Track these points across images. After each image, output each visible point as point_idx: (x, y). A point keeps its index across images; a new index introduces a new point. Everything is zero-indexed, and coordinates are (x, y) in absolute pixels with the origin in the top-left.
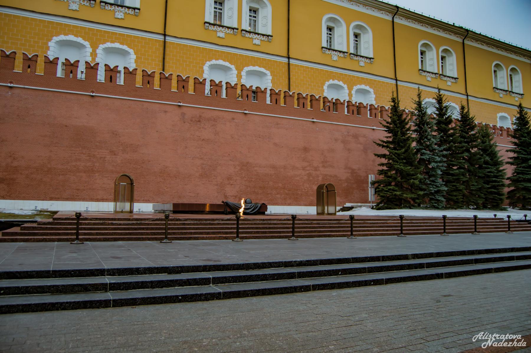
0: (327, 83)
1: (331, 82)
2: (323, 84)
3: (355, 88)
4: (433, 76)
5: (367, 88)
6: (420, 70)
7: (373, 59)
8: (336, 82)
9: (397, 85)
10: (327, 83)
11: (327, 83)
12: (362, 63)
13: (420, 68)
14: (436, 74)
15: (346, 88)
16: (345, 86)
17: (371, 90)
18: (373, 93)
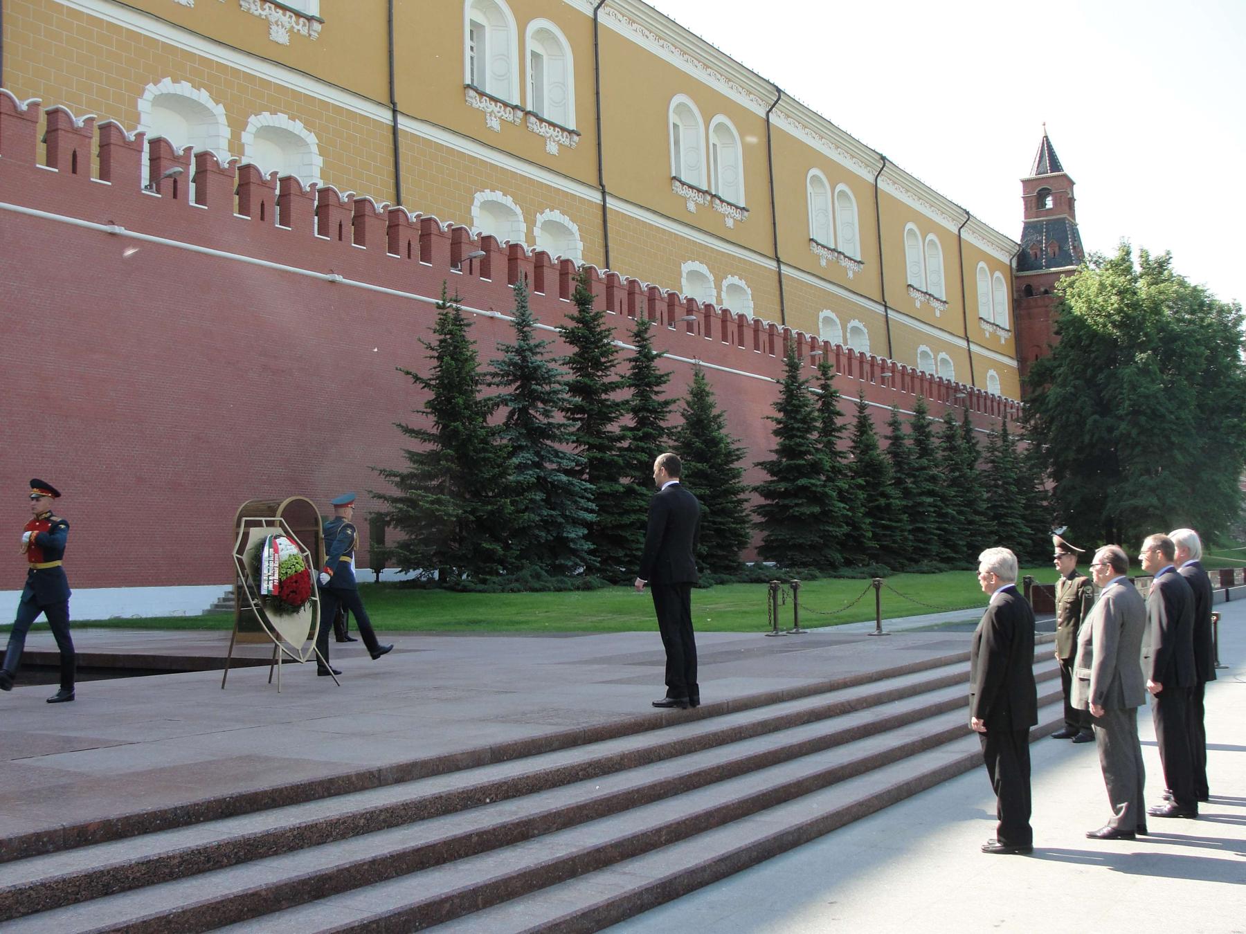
0: (150, 86)
1: (167, 86)
2: (141, 93)
3: (255, 122)
4: (508, 115)
5: (297, 127)
6: (468, 86)
7: (321, 22)
8: (185, 88)
9: (395, 130)
10: (150, 86)
11: (151, 90)
12: (282, 31)
13: (468, 82)
14: (515, 108)
15: (223, 120)
16: (219, 110)
17: (312, 139)
18: (315, 149)
